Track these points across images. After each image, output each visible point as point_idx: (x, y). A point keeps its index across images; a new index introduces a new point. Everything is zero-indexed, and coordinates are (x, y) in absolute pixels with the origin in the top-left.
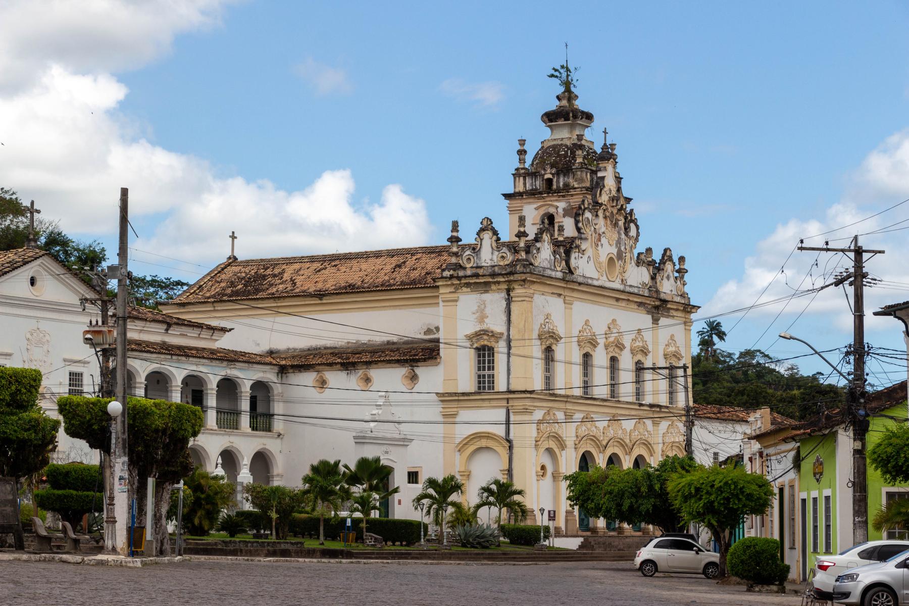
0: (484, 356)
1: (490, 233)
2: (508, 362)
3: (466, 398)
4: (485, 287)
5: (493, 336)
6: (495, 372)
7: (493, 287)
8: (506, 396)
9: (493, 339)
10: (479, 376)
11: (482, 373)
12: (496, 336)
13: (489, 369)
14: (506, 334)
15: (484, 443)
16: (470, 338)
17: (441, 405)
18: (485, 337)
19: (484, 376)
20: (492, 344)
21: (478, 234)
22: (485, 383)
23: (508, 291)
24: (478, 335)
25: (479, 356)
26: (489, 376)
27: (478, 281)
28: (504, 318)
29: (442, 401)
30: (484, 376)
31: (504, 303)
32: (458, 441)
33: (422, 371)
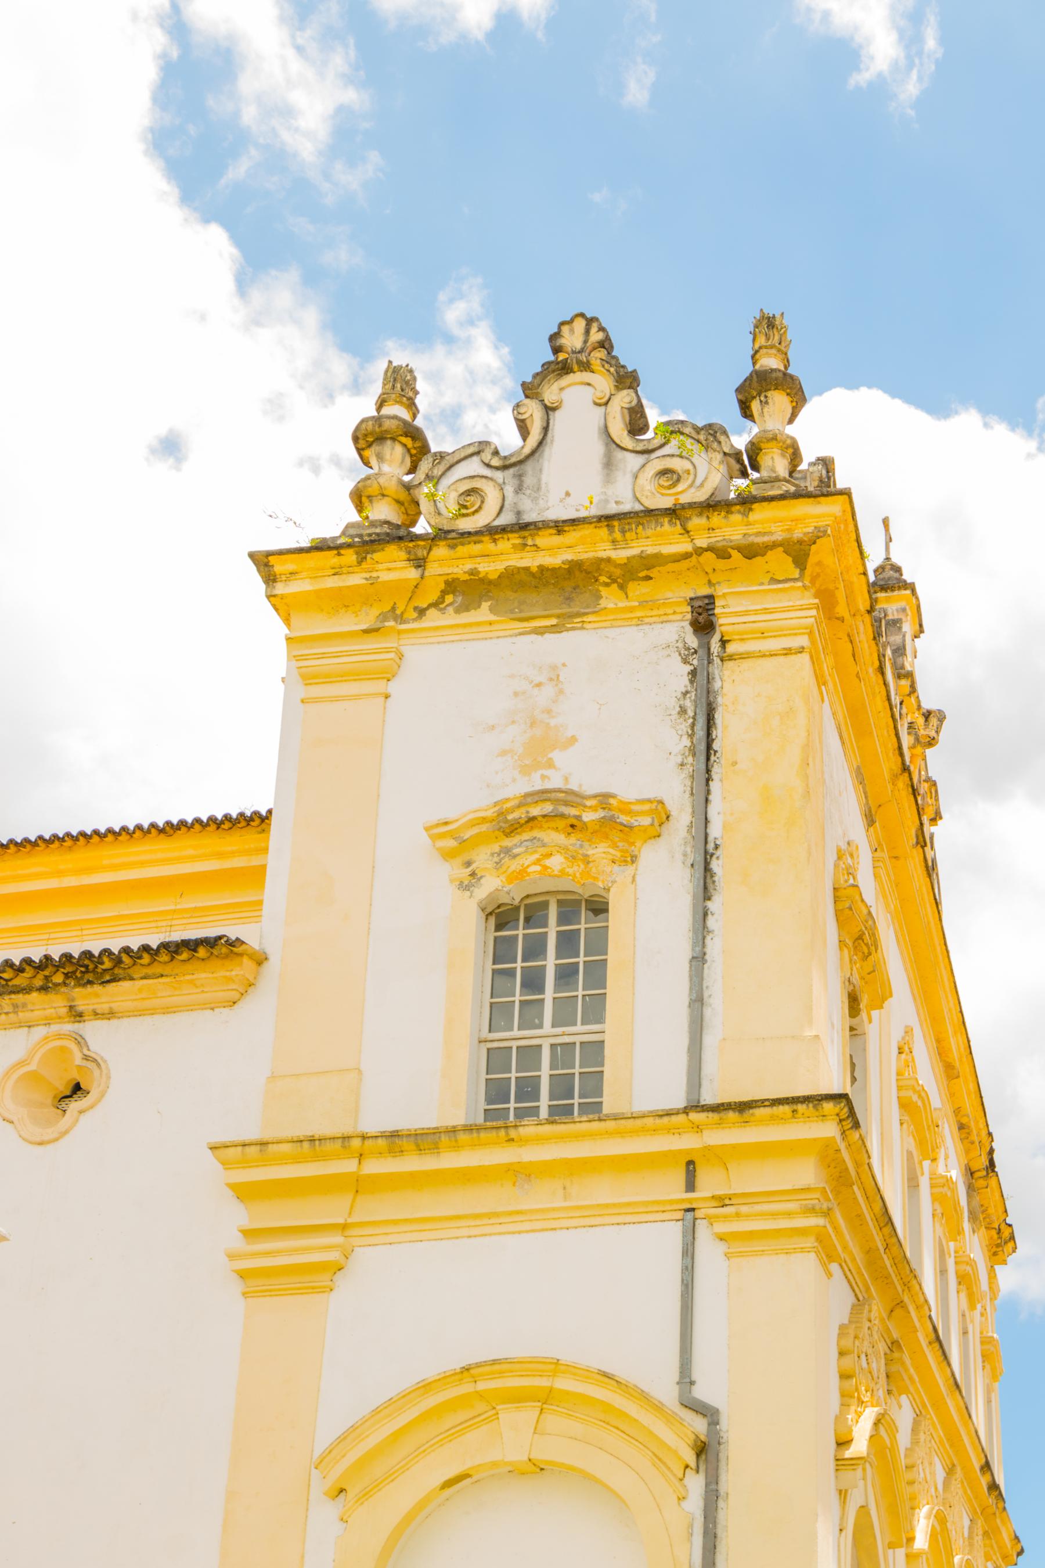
0: (535, 949)
1: (602, 382)
2: (699, 960)
3: (412, 1163)
4: (566, 591)
5: (609, 823)
6: (611, 1030)
7: (611, 598)
8: (687, 1143)
9: (600, 851)
10: (497, 1059)
11: (515, 1036)
12: (618, 825)
13: (564, 1016)
14: (683, 817)
15: (514, 1435)
16: (454, 842)
17: (238, 1216)
18: (553, 837)
19: (530, 1054)
20: (598, 867)
21: (530, 390)
22: (535, 1090)
23: (703, 620)
24: (510, 824)
25: (502, 951)
26: (562, 1052)
27: (530, 560)
28: (675, 740)
29: (244, 1193)
30: (530, 1054)
31: (677, 676)
32: (325, 1436)
33: (134, 1042)
